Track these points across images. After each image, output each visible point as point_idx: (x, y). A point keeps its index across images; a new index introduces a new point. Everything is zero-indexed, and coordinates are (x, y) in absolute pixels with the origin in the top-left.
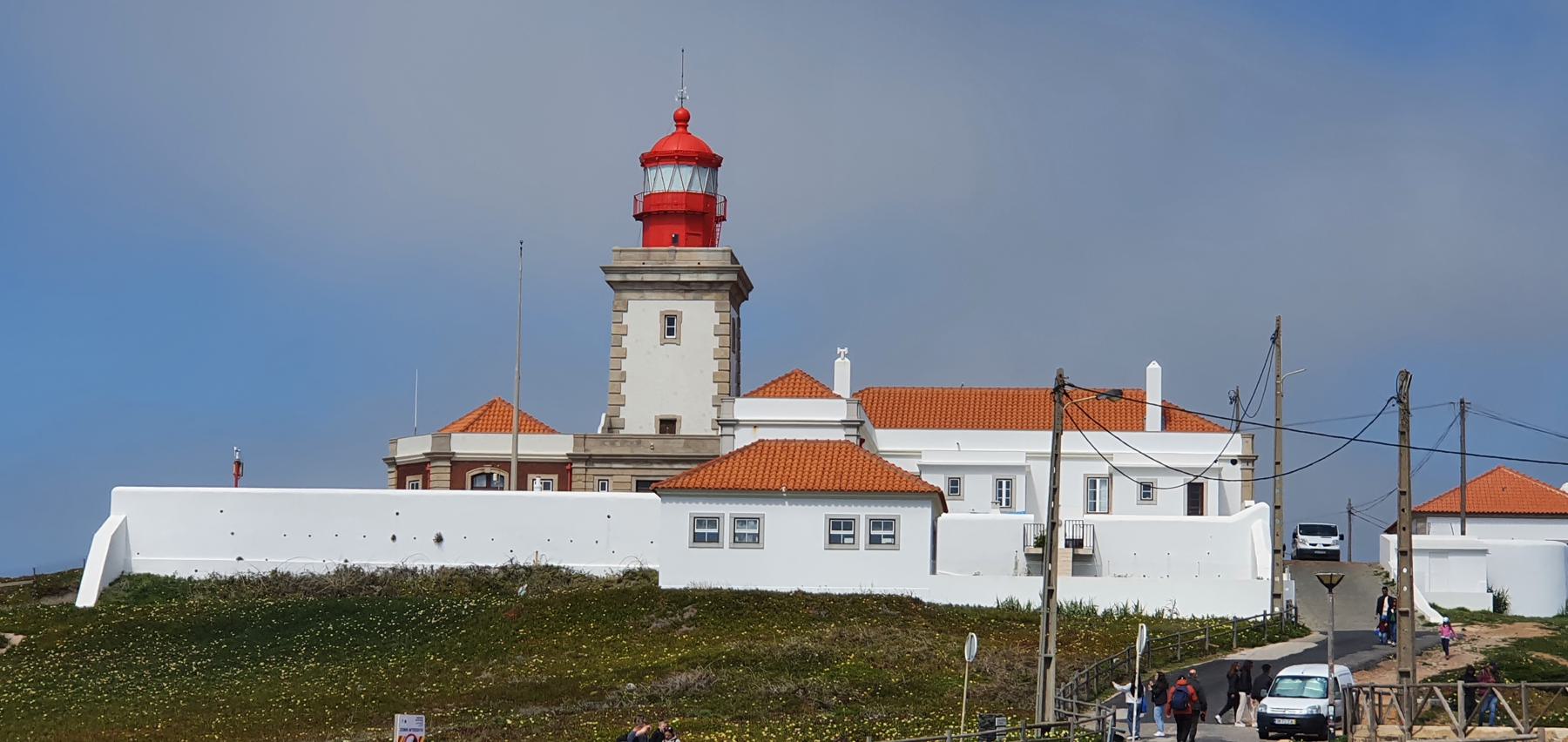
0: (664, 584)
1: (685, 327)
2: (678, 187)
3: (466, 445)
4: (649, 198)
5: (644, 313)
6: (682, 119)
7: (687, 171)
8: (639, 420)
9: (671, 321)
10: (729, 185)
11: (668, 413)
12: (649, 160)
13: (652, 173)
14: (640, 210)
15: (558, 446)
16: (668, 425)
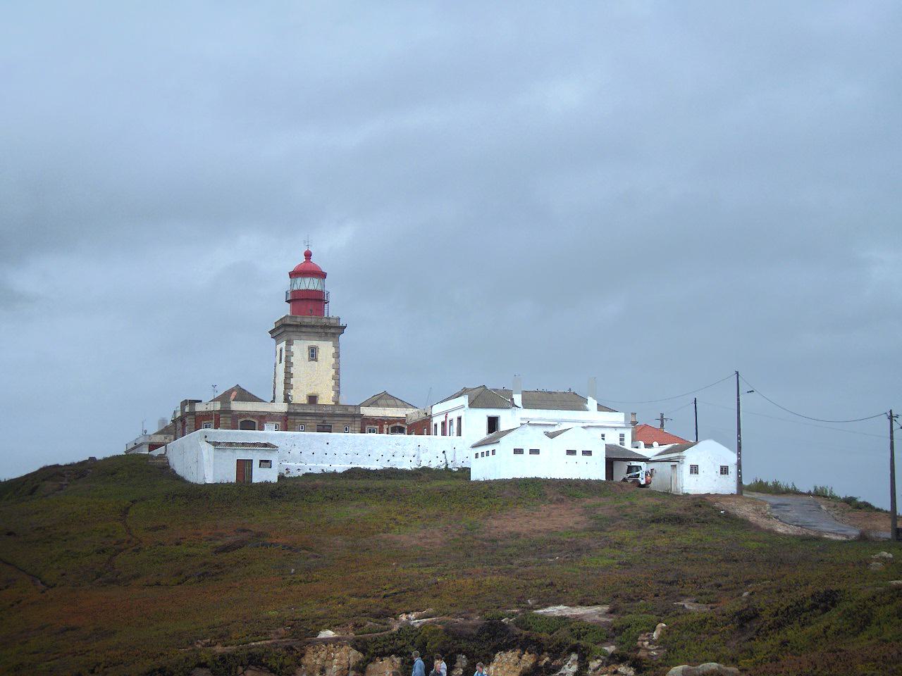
0: (474, 476)
1: (320, 356)
2: (311, 287)
3: (237, 406)
4: (294, 292)
5: (300, 348)
6: (308, 255)
7: (316, 280)
8: (299, 397)
9: (313, 351)
10: (331, 288)
11: (310, 392)
12: (294, 275)
13: (299, 280)
14: (289, 298)
15: (281, 407)
16: (313, 399)
